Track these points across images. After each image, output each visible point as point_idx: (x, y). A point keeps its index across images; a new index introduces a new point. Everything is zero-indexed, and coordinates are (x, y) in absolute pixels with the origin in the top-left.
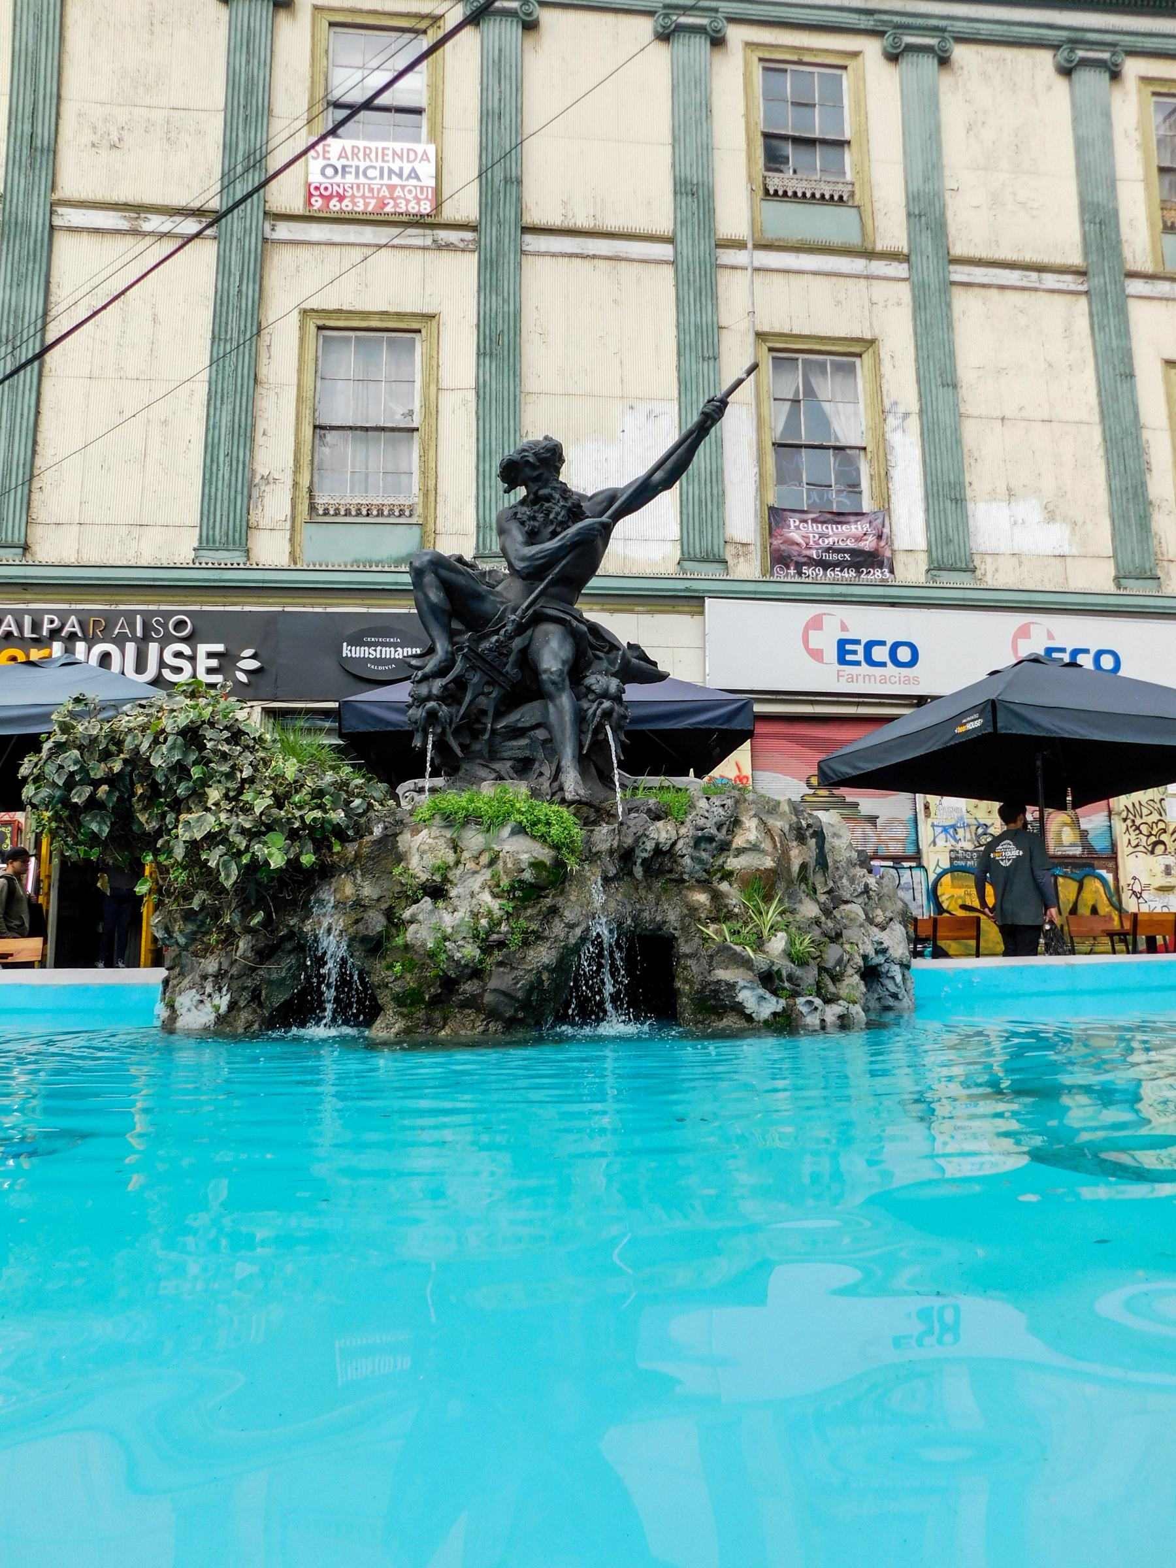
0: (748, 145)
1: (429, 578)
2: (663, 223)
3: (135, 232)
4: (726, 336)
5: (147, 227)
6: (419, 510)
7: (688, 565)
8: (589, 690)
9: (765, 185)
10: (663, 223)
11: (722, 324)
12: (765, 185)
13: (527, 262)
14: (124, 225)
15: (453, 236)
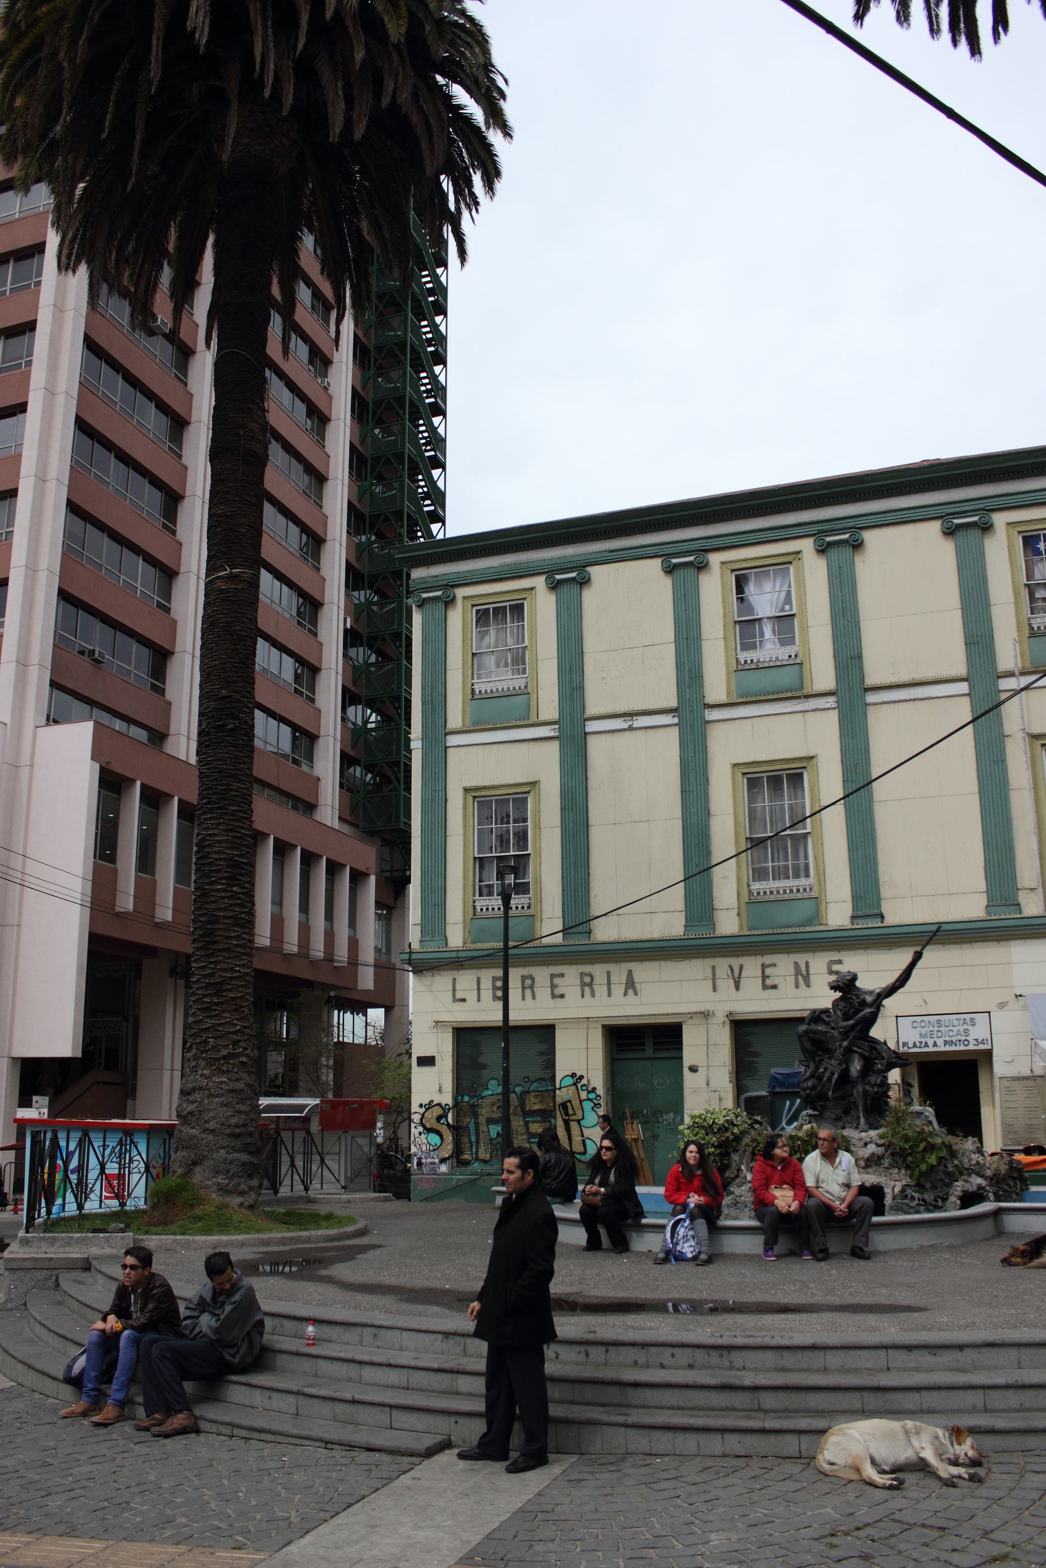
0: (1016, 599)
1: (804, 1038)
2: (961, 670)
3: (631, 728)
4: (1008, 742)
5: (636, 724)
6: (815, 888)
7: (991, 909)
8: (869, 1083)
9: (1030, 625)
10: (961, 670)
11: (1006, 734)
12: (1030, 625)
13: (870, 709)
14: (625, 726)
15: (821, 702)
